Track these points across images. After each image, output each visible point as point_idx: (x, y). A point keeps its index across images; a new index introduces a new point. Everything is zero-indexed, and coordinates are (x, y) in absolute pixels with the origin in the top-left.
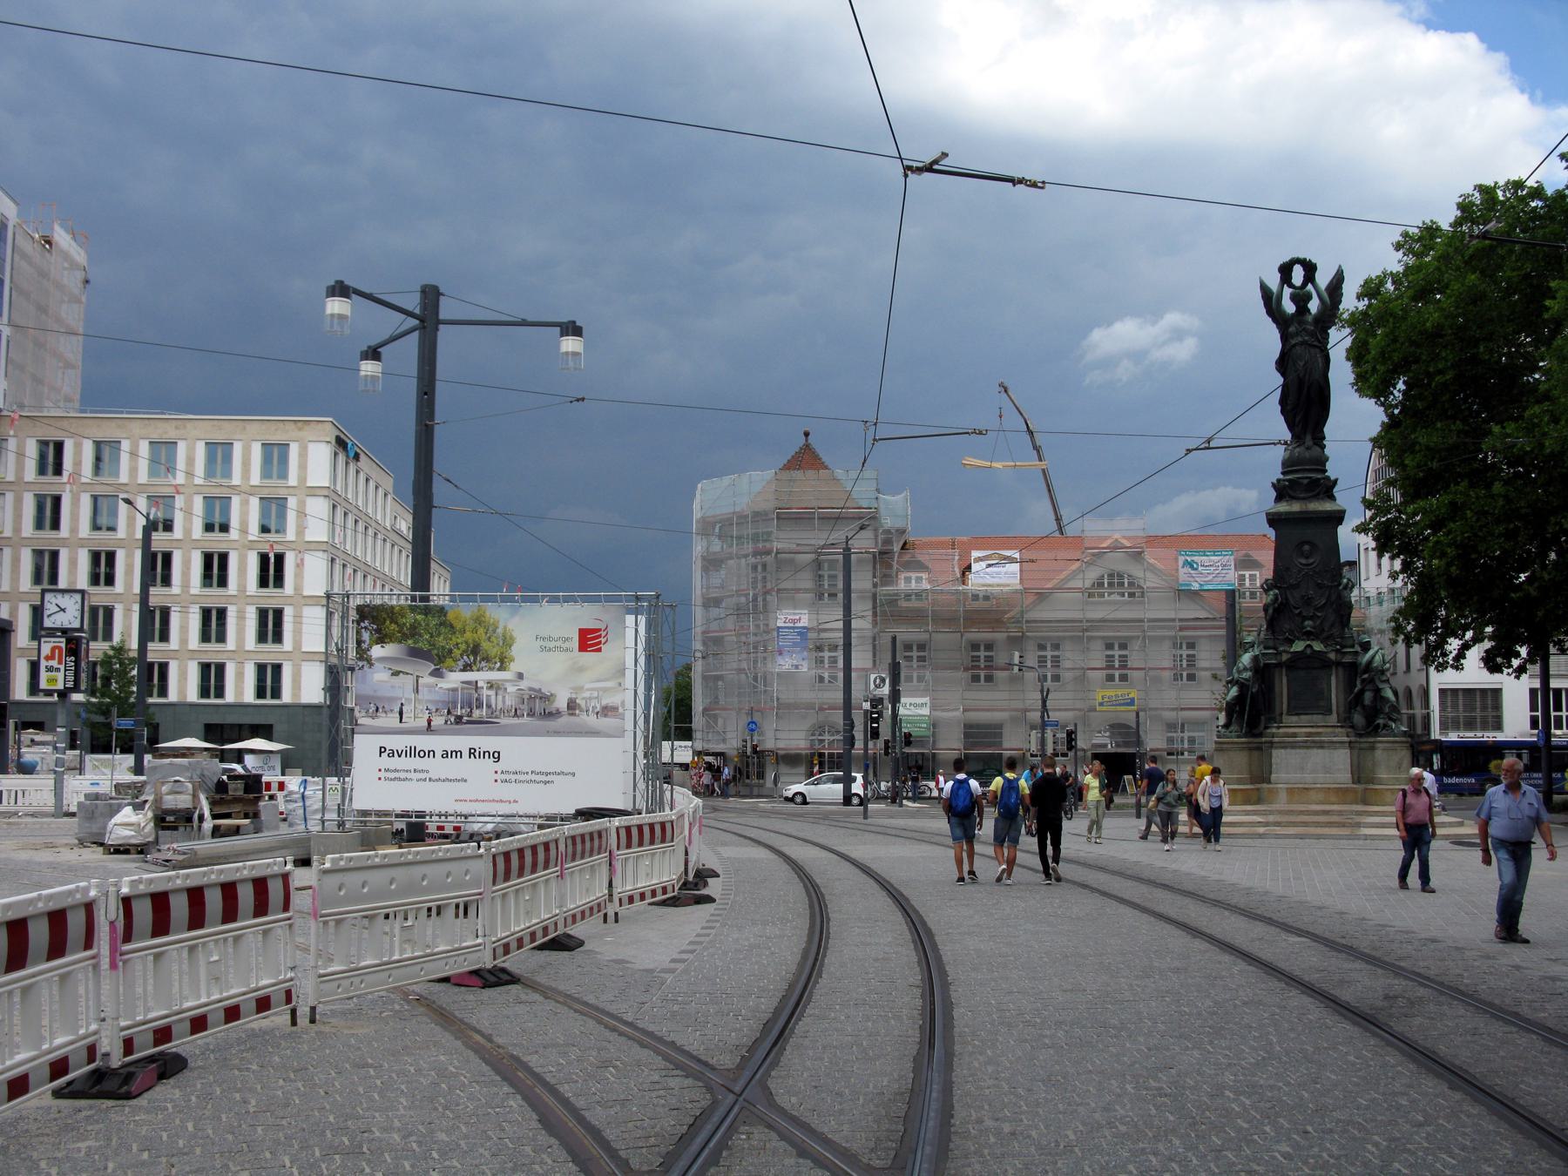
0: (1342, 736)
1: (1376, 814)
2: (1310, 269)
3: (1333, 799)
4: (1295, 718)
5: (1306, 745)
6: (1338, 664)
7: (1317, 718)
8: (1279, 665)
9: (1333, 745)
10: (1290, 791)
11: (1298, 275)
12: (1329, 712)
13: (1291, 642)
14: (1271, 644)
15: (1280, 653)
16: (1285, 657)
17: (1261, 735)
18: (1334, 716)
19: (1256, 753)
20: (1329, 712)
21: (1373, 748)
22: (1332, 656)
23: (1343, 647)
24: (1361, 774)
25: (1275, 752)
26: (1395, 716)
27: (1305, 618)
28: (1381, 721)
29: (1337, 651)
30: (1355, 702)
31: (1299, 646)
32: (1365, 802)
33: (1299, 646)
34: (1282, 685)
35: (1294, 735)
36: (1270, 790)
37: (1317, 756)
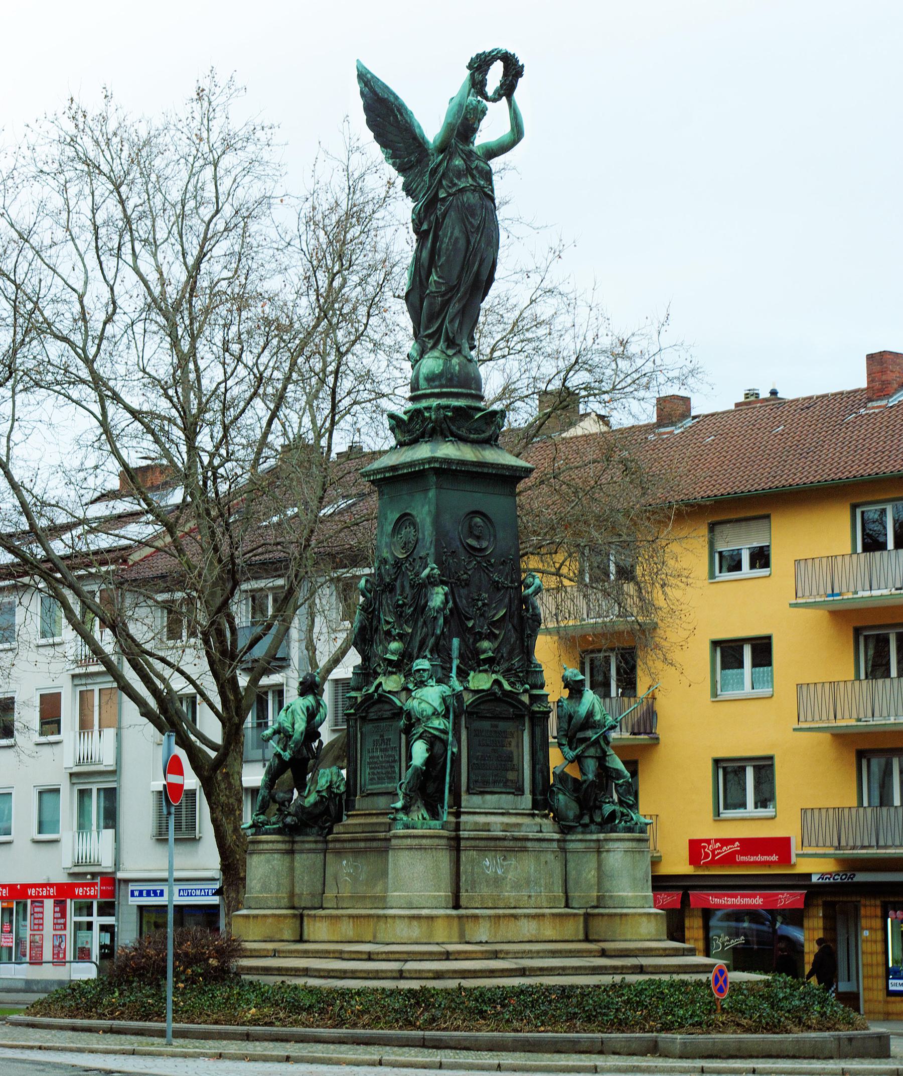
2: (513, 70)
4: (476, 800)
11: (495, 74)
20: (520, 791)
27: (480, 637)
35: (487, 827)
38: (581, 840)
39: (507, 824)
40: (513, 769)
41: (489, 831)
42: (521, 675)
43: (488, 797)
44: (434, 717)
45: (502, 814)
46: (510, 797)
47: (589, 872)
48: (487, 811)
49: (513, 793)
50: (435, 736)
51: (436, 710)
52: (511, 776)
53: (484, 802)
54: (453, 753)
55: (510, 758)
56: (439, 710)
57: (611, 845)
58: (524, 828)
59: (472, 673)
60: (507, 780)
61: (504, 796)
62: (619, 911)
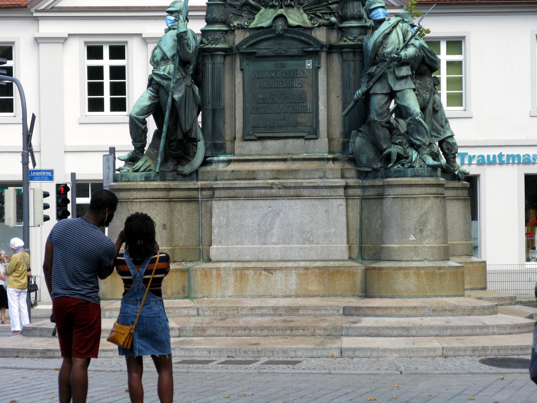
0: (334, 175)
1: (398, 311)
3: (314, 287)
4: (254, 147)
5: (268, 194)
6: (331, 49)
7: (293, 146)
8: (228, 52)
9: (318, 193)
10: (241, 274)
12: (314, 134)
13: (254, 10)
14: (217, 14)
15: (231, 31)
16: (239, 37)
17: (195, 175)
18: (320, 147)
19: (183, 209)
20: (314, 134)
21: (381, 197)
22: (321, 35)
23: (343, 19)
24: (369, 245)
25: (218, 207)
26: (419, 139)
28: (395, 150)
29: (331, 26)
30: (358, 115)
31: (264, 18)
32: (366, 294)
33: (264, 18)
34: (234, 86)
35: (252, 175)
36: (206, 273)
37: (295, 211)
38: (373, 186)
39: (279, 171)
40: (305, 111)
41: (254, 179)
42: (334, 6)
43: (270, 143)
44: (162, 62)
45: (285, 160)
46: (300, 142)
47: (377, 220)
48: (262, 157)
49: (302, 137)
50: (158, 83)
51: (164, 54)
52: (303, 119)
53: (264, 148)
54: (173, 100)
55: (302, 99)
56: (169, 54)
57: (390, 191)
58: (301, 175)
59: (263, 10)
60: (297, 124)
61: (290, 141)
62: (403, 264)
